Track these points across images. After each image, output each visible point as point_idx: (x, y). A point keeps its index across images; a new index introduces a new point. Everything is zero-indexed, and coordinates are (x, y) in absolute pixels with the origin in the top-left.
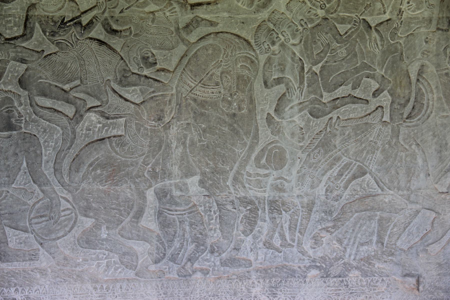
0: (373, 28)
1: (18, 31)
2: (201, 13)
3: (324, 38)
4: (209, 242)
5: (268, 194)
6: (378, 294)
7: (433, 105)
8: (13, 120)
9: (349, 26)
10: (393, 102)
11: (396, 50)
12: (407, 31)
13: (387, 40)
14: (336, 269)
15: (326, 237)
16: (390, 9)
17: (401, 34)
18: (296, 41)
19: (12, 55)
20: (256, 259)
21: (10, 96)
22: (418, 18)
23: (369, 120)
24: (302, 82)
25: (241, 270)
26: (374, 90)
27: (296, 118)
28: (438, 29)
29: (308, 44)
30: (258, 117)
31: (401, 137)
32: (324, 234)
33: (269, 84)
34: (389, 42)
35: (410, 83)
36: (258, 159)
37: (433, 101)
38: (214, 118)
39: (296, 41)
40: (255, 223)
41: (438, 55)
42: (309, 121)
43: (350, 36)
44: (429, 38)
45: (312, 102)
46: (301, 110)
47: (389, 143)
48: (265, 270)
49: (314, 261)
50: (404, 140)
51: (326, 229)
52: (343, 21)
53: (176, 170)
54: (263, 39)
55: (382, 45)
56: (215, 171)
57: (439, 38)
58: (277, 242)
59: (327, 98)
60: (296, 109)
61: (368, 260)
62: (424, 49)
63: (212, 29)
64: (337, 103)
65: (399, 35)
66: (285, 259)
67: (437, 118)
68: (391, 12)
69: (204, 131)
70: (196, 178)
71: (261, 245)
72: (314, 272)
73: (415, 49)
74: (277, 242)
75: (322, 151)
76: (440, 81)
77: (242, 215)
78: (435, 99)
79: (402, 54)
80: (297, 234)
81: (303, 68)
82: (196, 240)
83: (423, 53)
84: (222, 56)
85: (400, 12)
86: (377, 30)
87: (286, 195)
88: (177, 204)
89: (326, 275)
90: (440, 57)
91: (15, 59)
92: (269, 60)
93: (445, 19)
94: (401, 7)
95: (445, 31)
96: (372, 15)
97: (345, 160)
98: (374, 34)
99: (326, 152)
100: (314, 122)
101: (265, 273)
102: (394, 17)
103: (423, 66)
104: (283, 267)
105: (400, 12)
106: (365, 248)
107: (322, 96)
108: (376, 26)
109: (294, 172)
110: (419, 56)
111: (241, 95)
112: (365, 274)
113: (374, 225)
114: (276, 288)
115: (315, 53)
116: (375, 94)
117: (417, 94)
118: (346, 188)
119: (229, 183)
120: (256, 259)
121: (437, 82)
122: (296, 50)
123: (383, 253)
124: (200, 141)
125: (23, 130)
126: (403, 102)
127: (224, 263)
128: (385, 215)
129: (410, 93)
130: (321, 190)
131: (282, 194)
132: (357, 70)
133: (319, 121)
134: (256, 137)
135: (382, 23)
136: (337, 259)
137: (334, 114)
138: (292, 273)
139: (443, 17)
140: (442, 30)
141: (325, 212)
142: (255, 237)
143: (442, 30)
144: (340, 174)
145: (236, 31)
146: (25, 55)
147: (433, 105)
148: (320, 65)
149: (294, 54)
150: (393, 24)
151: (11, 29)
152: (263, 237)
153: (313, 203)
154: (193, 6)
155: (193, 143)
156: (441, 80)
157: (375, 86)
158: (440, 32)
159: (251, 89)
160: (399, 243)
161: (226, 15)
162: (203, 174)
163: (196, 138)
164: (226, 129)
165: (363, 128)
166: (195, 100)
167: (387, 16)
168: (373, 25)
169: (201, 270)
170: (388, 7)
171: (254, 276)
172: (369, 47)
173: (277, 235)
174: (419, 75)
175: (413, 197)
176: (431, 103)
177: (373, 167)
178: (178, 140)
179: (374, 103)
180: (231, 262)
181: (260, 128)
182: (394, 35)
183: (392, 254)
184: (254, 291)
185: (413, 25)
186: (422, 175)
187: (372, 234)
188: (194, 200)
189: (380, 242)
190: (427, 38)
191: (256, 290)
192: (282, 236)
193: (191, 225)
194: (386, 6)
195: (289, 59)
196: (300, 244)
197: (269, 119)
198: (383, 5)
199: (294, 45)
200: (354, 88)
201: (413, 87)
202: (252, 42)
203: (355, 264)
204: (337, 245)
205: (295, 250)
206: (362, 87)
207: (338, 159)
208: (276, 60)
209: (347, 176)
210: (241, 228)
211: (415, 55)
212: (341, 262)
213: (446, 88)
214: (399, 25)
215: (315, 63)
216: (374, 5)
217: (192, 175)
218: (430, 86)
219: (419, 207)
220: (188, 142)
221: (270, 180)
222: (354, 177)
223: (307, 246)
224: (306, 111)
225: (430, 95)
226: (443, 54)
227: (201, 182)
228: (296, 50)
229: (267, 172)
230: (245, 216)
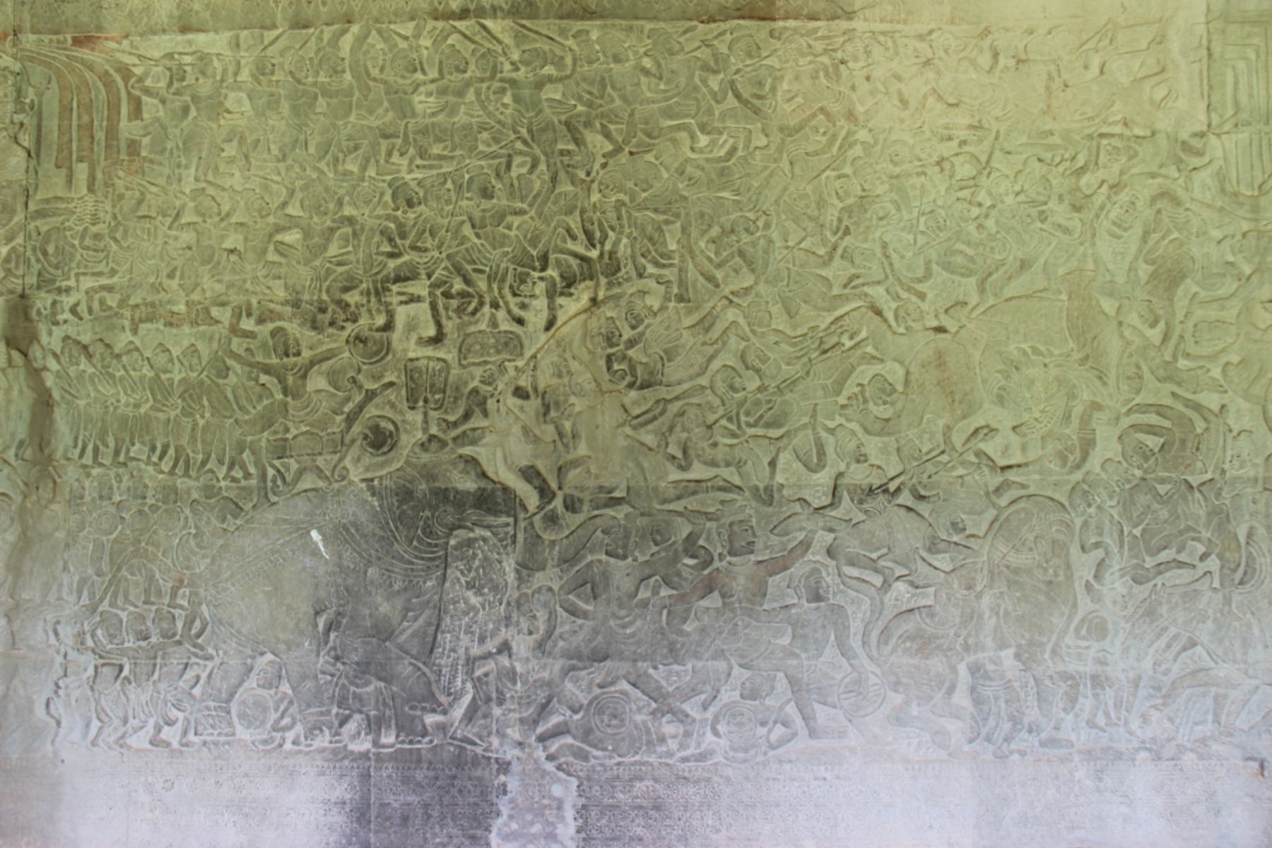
1: (826, 500)
2: (1011, 476)
3: (1143, 499)
4: (1026, 720)
5: (1089, 668)
6: (1217, 780)
8: (821, 591)
9: (1169, 487)
10: (1222, 567)
11: (1222, 511)
14: (1169, 751)
15: (1155, 715)
18: (1113, 503)
19: (821, 524)
20: (1078, 740)
21: (818, 566)
23: (1197, 586)
24: (1122, 546)
25: (1062, 752)
26: (1200, 554)
27: (1117, 585)
28: (1266, 489)
29: (1127, 504)
30: (1077, 584)
31: (1234, 606)
32: (1153, 712)
35: (1239, 546)
36: (1077, 630)
39: (1113, 503)
40: (1077, 699)
42: (1131, 588)
43: (1171, 497)
45: (1135, 567)
46: (1122, 576)
47: (1221, 611)
48: (1089, 752)
49: (1143, 742)
50: (1237, 608)
51: (1155, 707)
52: (1162, 481)
53: (989, 642)
54: (1078, 501)
56: (1031, 643)
58: (1101, 721)
59: (1149, 562)
60: (1117, 575)
61: (1203, 741)
63: (1023, 492)
64: (1161, 568)
66: (1111, 739)
69: (1019, 599)
70: (1010, 652)
71: (1083, 724)
72: (1143, 755)
74: (1101, 721)
75: (1148, 620)
77: (1061, 691)
80: (1124, 712)
81: (1122, 531)
82: (1012, 718)
83: (1251, 515)
85: (1223, 472)
86: (1200, 492)
87: (1109, 669)
88: (991, 679)
89: (1158, 758)
91: (823, 529)
92: (1085, 524)
97: (1173, 630)
98: (1197, 495)
99: (1152, 622)
100: (1137, 589)
101: (1089, 755)
102: (1217, 477)
103: (1251, 528)
104: (1110, 748)
106: (1199, 728)
109: (1118, 642)
110: (1247, 517)
111: (1055, 561)
112: (1201, 757)
113: (1209, 702)
114: (1102, 771)
116: (1203, 557)
117: (1247, 558)
118: (1175, 660)
119: (1047, 656)
120: (1078, 740)
122: (1115, 513)
123: (1221, 733)
124: (1015, 610)
125: (831, 601)
126: (1233, 566)
127: (1042, 744)
128: (1221, 691)
129: (1240, 557)
130: (1147, 664)
131: (1105, 668)
132: (1181, 533)
133: (1142, 588)
134: (1075, 605)
136: (1169, 740)
137: (1159, 581)
138: (1119, 755)
141: (1153, 688)
142: (1076, 716)
144: (1169, 646)
145: (1049, 494)
146: (833, 524)
148: (1140, 528)
151: (819, 498)
152: (1085, 716)
153: (1140, 678)
154: (1003, 469)
155: (1007, 613)
157: (1201, 549)
159: (1067, 555)
160: (1238, 722)
161: (1037, 477)
162: (1019, 646)
163: (1010, 608)
164: (1042, 598)
165: (1191, 595)
166: (1008, 567)
167: (1208, 476)
168: (1195, 485)
169: (1019, 752)
171: (1077, 758)
173: (1100, 713)
175: (1251, 671)
177: (1204, 638)
178: (992, 610)
179: (1202, 567)
180: (1051, 743)
181: (1079, 597)
182: (1218, 495)
183: (1231, 735)
184: (1078, 775)
186: (1260, 647)
187: (1206, 712)
188: (1009, 675)
189: (1217, 721)
191: (1080, 774)
192: (1107, 714)
193: (1007, 702)
196: (1126, 723)
197: (1088, 586)
199: (1112, 507)
200: (1179, 552)
201: (1243, 550)
202: (1067, 504)
203: (1189, 745)
204: (1168, 725)
205: (1121, 729)
206: (1187, 551)
207: (1165, 629)
208: (1093, 522)
209: (1176, 647)
210: (1061, 705)
212: (1173, 743)
215: (1136, 526)
217: (1007, 647)
219: (1257, 682)
220: (1002, 612)
221: (1092, 653)
222: (1184, 649)
223: (1135, 725)
224: (1128, 578)
227: (1017, 656)
228: (1115, 513)
229: (1087, 644)
230: (1066, 693)
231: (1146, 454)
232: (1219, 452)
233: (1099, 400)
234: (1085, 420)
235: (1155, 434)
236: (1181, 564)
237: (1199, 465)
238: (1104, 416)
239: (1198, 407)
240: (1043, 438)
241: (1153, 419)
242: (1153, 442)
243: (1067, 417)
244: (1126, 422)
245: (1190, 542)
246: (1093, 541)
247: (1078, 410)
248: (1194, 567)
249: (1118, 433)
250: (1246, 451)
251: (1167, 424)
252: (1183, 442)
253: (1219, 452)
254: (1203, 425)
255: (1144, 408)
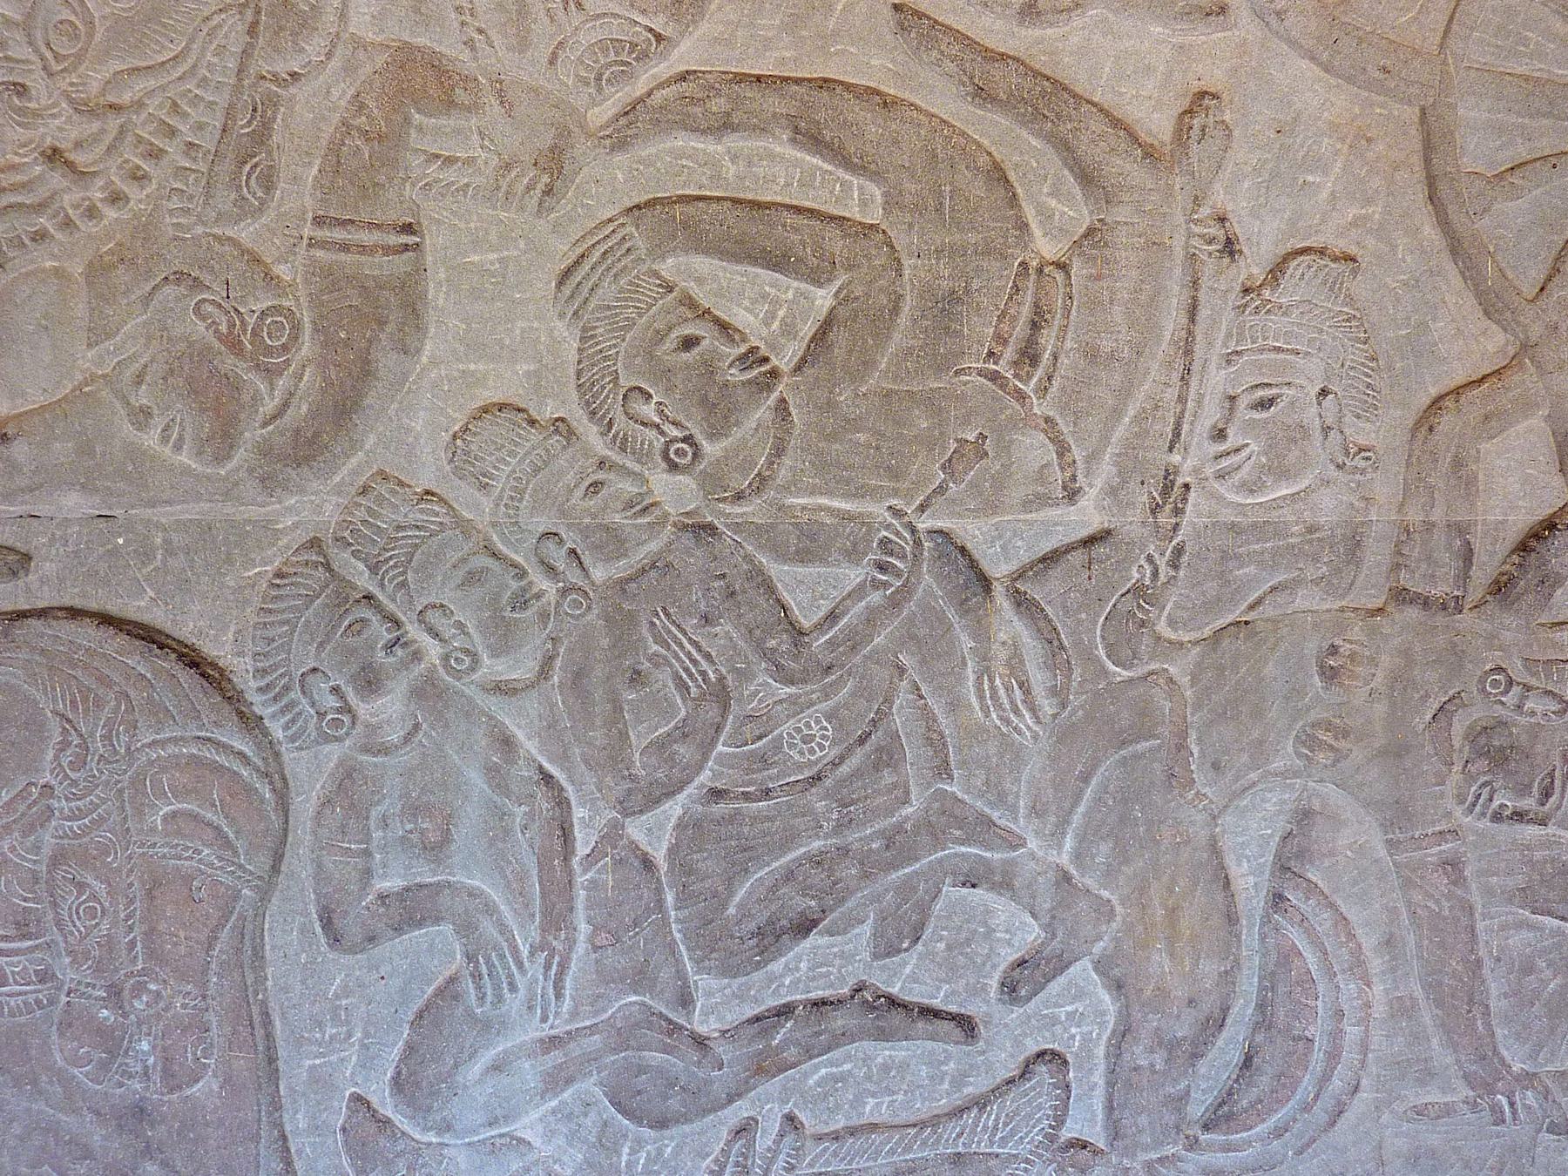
0: (998, 589)
7: (1364, 1048)
9: (854, 575)
10: (1123, 1034)
12: (1213, 605)
13: (1090, 658)
16: (1106, 469)
17: (1172, 623)
18: (521, 668)
22: (1279, 530)
24: (556, 919)
26: (1010, 955)
27: (528, 1126)
28: (1401, 596)
30: (297, 1121)
33: (351, 928)
34: (1105, 672)
35: (1231, 919)
37: (1365, 1021)
38: (17, 1129)
39: (521, 668)
41: (1397, 751)
42: (607, 1142)
43: (854, 641)
44: (1346, 648)
45: (623, 1036)
46: (555, 1081)
52: (809, 545)
55: (1053, 691)
57: (1406, 653)
59: (717, 1005)
60: (529, 1072)
62: (1313, 716)
65: (1162, 628)
67: (1385, 1118)
68: (1112, 491)
73: (1258, 714)
76: (1409, 903)
78: (1379, 1010)
79: (1181, 747)
83: (1309, 741)
84: (50, 755)
86: (1022, 602)
90: (1408, 764)
93: (1439, 537)
94: (1176, 458)
95: (1444, 607)
96: (991, 507)
98: (1008, 625)
102: (1132, 523)
103: (1304, 816)
105: (1167, 490)
107: (685, 1000)
108: (1020, 575)
115: (639, 738)
116: (1022, 979)
117: (1269, 981)
121: (1394, 911)
129: (1228, 977)
135: (1051, 559)
137: (766, 1105)
139: (1429, 526)
140: (1426, 603)
143: (1426, 603)
147: (1364, 1048)
148: (674, 808)
149: (507, 743)
150: (1123, 565)
156: (1417, 897)
157: (1017, 930)
158: (1413, 613)
161: (74, 503)
167: (1087, 515)
168: (999, 569)
170: (1092, 458)
172: (974, 700)
174: (1283, 868)
176: (1352, 1032)
179: (1010, 1035)
182: (1129, 627)
185: (1251, 569)
190: (1334, 650)
194: (1077, 454)
195: (475, 777)
198: (1062, 450)
199: (502, 689)
200: (886, 948)
201: (1250, 936)
206: (936, 939)
211: (1260, 753)
213: (1442, 945)
214: (1164, 571)
216: (1005, 448)
218: (1351, 936)
224: (590, 1085)
225: (1349, 988)
226: (1429, 749)
231: (719, 379)
232: (1155, 380)
233: (449, 47)
234: (366, 156)
235: (778, 262)
236: (890, 1012)
237: (1034, 449)
238: (473, 141)
239: (1046, 100)
240: (97, 270)
241: (779, 168)
242: (768, 308)
243: (248, 150)
244: (607, 183)
245: (951, 892)
246: (391, 883)
247: (318, 104)
248: (966, 1025)
249: (562, 251)
250: (1311, 373)
251: (861, 199)
252: (946, 308)
253: (1155, 380)
254: (1077, 213)
255: (722, 102)
